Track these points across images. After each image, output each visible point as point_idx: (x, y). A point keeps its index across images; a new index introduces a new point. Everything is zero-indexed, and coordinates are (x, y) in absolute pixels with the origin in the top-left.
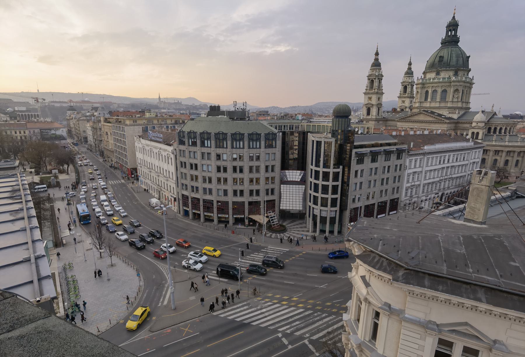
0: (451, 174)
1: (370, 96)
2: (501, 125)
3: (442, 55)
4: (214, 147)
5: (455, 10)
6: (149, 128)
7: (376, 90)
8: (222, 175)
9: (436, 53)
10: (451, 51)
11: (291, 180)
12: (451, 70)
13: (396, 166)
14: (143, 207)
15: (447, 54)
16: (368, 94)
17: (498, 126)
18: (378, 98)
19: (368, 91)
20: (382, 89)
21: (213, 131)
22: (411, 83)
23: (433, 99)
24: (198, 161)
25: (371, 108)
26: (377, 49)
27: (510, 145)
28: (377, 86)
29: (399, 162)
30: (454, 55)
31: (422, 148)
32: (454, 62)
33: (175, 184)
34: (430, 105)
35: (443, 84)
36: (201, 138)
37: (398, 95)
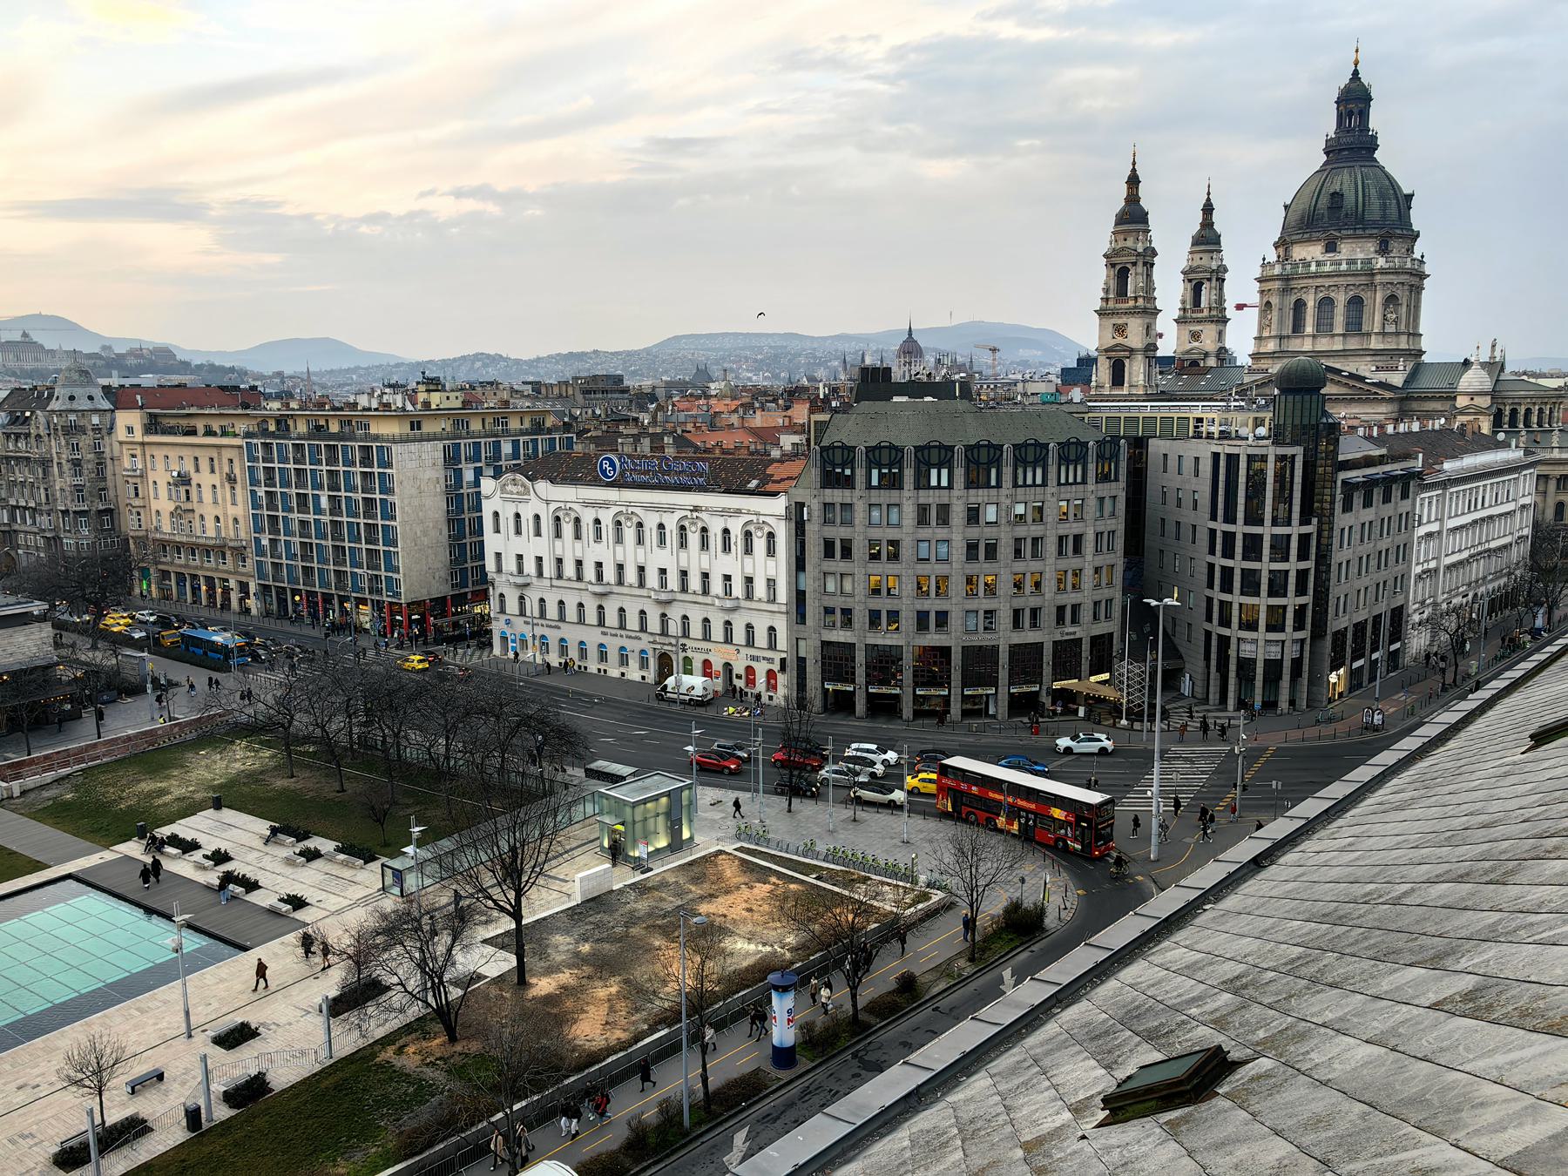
2: (1529, 400)
5: (1357, 51)
7: (1141, 301)
8: (982, 567)
10: (1362, 177)
12: (1371, 236)
15: (1353, 185)
16: (1114, 313)
17: (1520, 404)
22: (1217, 271)
23: (1324, 326)
24: (906, 529)
25: (1127, 362)
29: (1404, 506)
30: (1373, 191)
31: (1436, 467)
32: (1374, 212)
35: (1351, 280)
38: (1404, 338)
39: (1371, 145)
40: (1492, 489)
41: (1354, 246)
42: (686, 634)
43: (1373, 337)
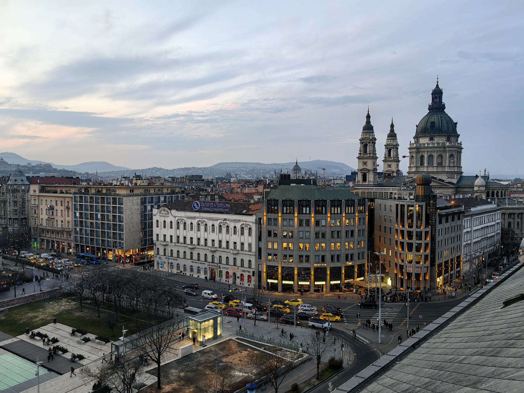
2: (497, 189)
5: (438, 79)
7: (371, 154)
12: (444, 136)
13: (446, 228)
15: (438, 120)
16: (363, 158)
19: (362, 155)
23: (430, 164)
25: (367, 174)
26: (368, 111)
27: (510, 208)
28: (372, 150)
29: (459, 222)
30: (444, 122)
35: (438, 149)
38: (456, 168)
39: (443, 107)
40: (487, 217)
42: (220, 263)
43: (446, 167)
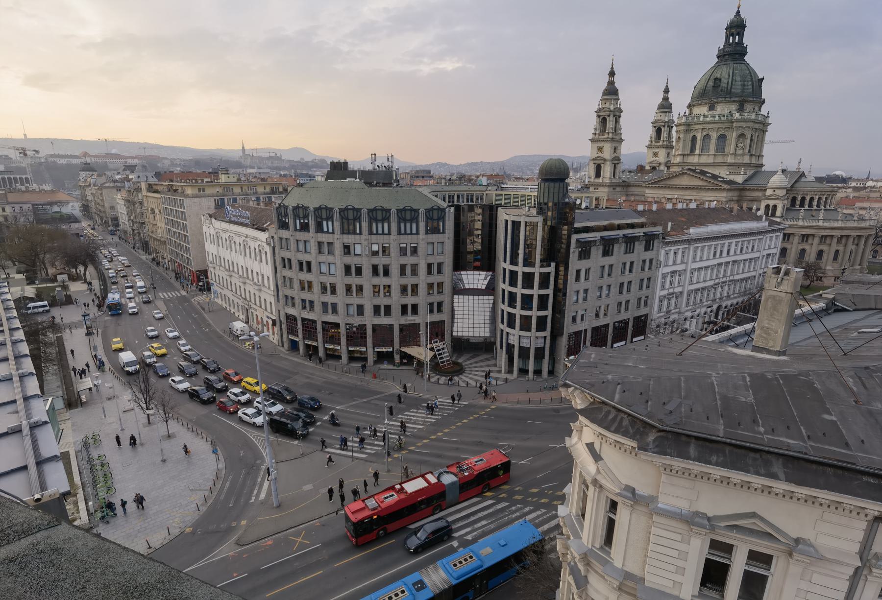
0: (732, 275)
1: (601, 145)
2: (813, 193)
3: (718, 77)
4: (339, 232)
6: (226, 200)
7: (611, 135)
8: (354, 280)
9: (709, 74)
11: (471, 287)
12: (734, 101)
13: (644, 261)
14: (221, 337)
15: (727, 74)
16: (598, 141)
17: (807, 194)
18: (613, 148)
19: (597, 136)
20: (621, 134)
21: (337, 205)
22: (668, 122)
24: (312, 256)
25: (602, 165)
27: (825, 226)
29: (648, 255)
30: (738, 77)
31: (686, 231)
32: (737, 88)
33: (274, 296)
34: (699, 160)
35: (720, 125)
36: (317, 217)
37: (648, 143)
41: (724, 107)
